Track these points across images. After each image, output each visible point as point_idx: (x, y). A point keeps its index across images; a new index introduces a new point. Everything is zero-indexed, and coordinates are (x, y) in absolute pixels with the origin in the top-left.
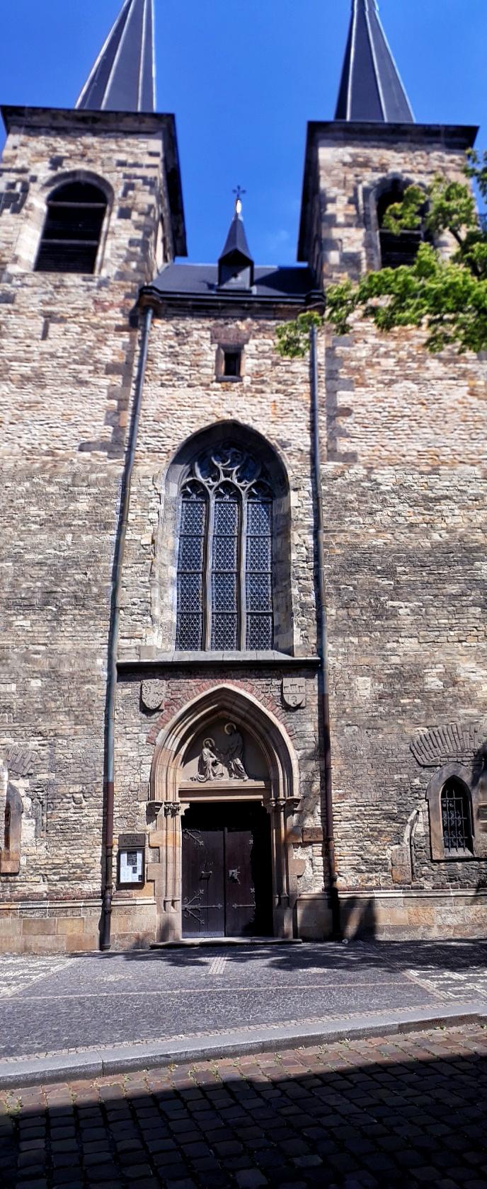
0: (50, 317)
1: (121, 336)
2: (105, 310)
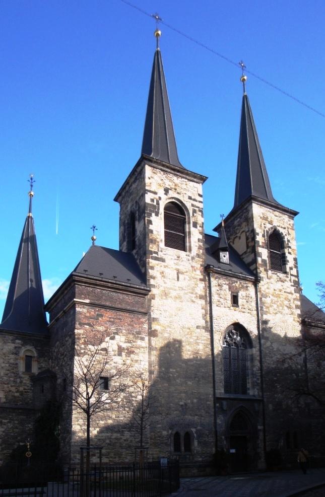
0: (179, 272)
1: (202, 283)
2: (195, 270)
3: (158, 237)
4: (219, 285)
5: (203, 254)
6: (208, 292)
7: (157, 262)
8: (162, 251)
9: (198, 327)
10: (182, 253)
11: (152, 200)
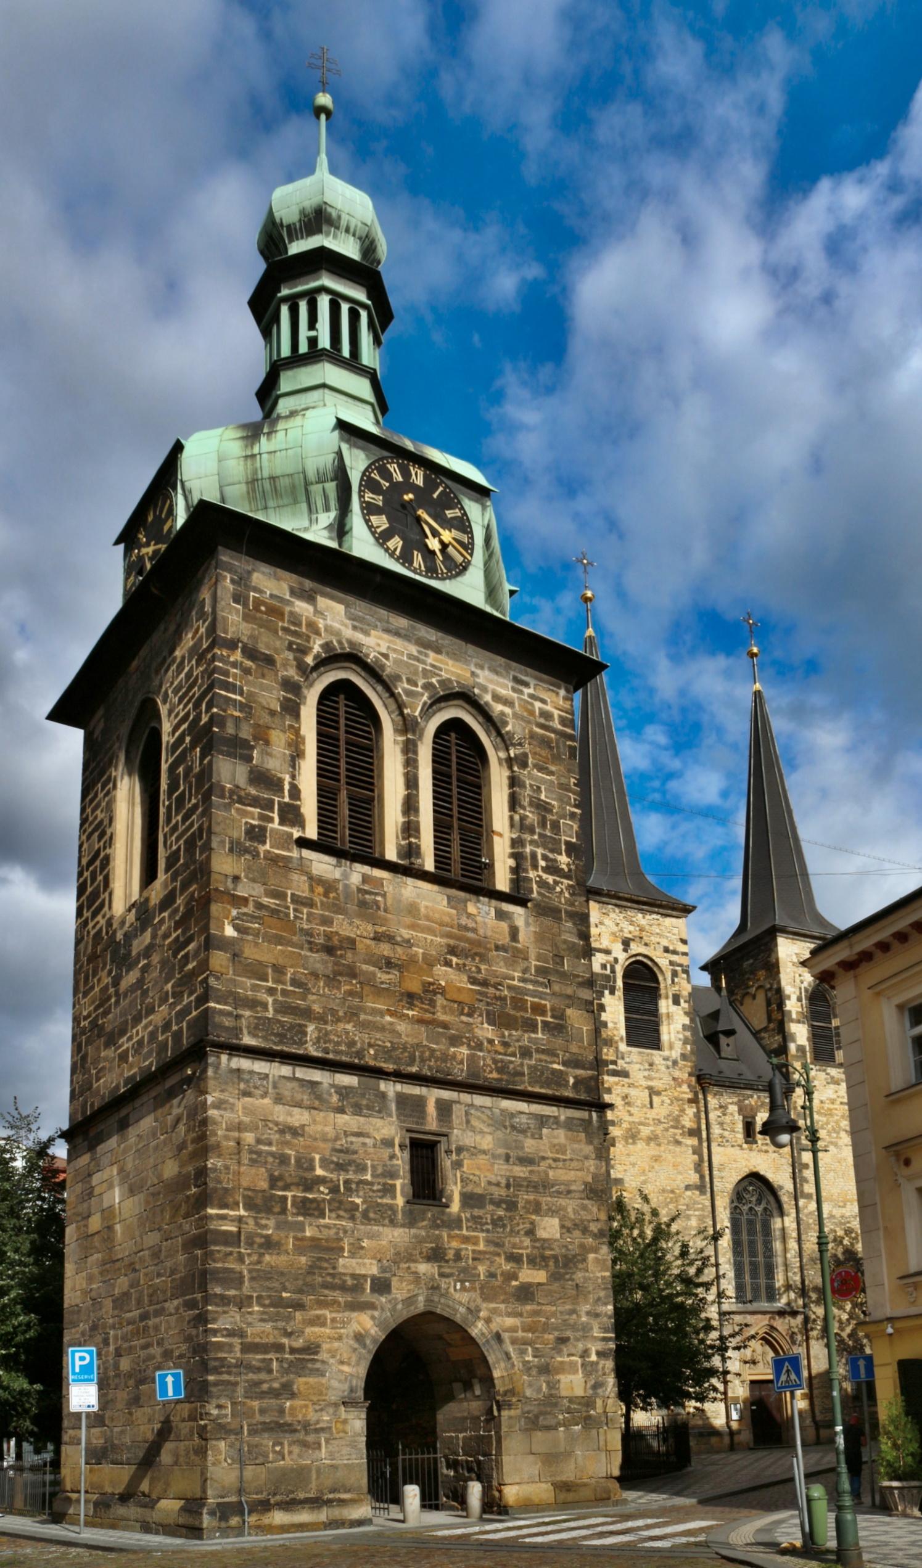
0: (653, 1092)
3: (615, 1032)
4: (721, 1107)
5: (692, 1051)
6: (703, 1121)
7: (616, 1079)
8: (623, 1058)
9: (688, 1188)
10: (656, 1056)
11: (604, 966)
